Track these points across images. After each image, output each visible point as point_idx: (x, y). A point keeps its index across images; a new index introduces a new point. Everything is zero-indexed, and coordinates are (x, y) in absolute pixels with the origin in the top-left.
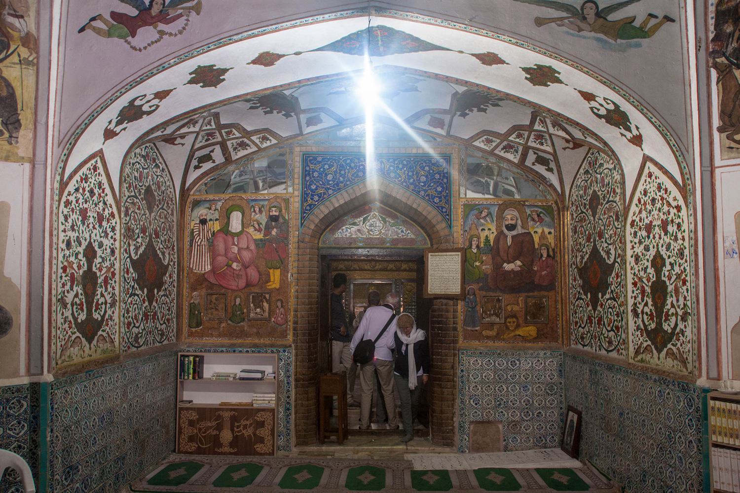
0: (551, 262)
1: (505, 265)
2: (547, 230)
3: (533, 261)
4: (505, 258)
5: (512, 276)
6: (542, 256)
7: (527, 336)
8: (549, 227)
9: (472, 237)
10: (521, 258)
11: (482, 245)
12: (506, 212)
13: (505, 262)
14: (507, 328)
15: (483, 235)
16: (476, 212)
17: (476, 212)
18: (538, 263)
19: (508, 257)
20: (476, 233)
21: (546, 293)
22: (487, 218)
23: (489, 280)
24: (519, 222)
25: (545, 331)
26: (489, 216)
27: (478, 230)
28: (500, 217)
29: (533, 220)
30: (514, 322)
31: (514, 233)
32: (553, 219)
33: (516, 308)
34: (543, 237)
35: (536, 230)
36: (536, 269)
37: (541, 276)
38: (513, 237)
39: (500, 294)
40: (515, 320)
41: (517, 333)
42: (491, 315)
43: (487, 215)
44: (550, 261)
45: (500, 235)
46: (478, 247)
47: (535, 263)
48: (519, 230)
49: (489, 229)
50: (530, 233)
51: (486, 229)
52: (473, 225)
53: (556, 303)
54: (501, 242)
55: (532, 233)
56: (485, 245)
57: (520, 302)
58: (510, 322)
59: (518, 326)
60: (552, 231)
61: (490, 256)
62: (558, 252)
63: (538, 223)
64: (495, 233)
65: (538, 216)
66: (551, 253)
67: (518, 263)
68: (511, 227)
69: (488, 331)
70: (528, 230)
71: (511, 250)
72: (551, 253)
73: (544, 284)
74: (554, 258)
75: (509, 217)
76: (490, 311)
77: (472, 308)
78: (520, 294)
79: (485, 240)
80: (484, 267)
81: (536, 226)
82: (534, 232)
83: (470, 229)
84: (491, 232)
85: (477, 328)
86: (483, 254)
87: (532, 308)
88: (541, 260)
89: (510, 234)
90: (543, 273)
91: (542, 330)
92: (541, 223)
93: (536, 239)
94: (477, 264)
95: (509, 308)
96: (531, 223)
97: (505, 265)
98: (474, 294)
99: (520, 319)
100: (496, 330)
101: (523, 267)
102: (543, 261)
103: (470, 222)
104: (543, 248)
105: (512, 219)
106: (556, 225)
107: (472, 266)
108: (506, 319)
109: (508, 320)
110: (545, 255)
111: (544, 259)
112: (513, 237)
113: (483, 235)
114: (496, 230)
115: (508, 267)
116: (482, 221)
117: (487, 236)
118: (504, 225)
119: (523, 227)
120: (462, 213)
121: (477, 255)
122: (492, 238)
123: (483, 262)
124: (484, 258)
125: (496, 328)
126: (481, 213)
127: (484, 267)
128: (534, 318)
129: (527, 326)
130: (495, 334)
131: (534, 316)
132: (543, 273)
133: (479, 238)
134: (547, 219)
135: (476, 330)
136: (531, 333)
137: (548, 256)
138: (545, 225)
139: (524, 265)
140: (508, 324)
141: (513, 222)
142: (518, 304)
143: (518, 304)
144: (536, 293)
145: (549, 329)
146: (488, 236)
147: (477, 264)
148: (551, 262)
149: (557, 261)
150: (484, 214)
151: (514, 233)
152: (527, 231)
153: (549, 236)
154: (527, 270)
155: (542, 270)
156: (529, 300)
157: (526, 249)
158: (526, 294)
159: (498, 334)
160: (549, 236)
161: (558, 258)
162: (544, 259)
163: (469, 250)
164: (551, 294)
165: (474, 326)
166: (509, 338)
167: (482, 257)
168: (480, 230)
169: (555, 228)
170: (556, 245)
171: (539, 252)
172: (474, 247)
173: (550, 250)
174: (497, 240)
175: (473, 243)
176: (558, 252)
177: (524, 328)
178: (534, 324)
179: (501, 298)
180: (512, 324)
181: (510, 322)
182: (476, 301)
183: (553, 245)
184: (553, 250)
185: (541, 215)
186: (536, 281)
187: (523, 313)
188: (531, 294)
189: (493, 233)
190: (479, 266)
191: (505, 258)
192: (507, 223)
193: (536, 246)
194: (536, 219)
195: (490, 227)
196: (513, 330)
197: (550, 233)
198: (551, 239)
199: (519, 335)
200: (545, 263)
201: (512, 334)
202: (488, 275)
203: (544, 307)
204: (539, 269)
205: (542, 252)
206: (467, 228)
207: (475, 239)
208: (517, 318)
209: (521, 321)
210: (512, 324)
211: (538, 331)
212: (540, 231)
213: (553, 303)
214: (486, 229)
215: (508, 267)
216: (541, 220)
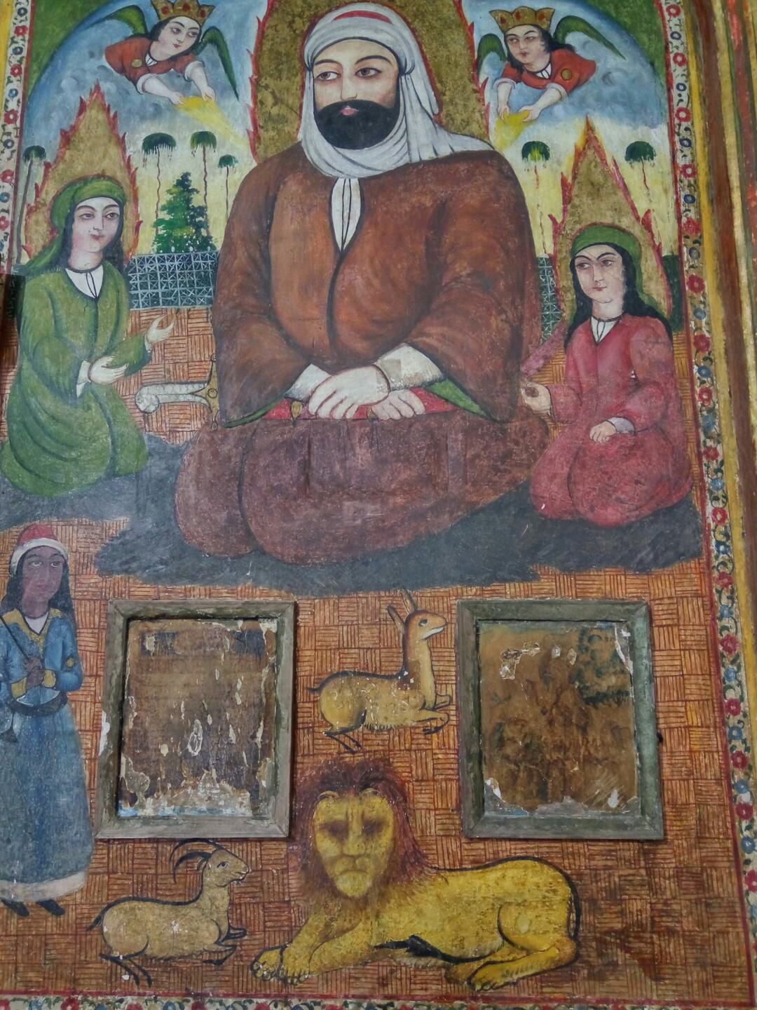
0: (657, 352)
1: (311, 378)
2: (615, 136)
3: (514, 351)
4: (316, 332)
5: (362, 456)
6: (585, 308)
7: (484, 958)
8: (633, 109)
9: (74, 190)
10: (434, 332)
11: (146, 244)
12: (327, 27)
13: (309, 357)
14: (319, 879)
15: (154, 183)
16: (115, 32)
17: (115, 32)
18: (560, 362)
19: (331, 328)
20: (110, 162)
21: (629, 586)
22: (193, 70)
23: (188, 491)
24: (418, 86)
25: (638, 906)
26: (210, 52)
27: (121, 143)
28: (285, 56)
29: (516, 70)
30: (372, 828)
31: (381, 157)
32: (659, 62)
33: (390, 707)
34: (588, 174)
35: (538, 133)
36: (541, 402)
37: (581, 455)
38: (372, 187)
39: (265, 595)
40: (378, 805)
41: (401, 921)
42: (170, 778)
43: (194, 50)
44: (648, 347)
45: (282, 169)
46: (113, 255)
47: (534, 363)
48: (417, 138)
49: (204, 138)
50: (492, 158)
51: (183, 138)
52: (94, 114)
53: (717, 660)
54: (287, 222)
55: (512, 155)
56: (164, 243)
57: (421, 654)
58: (338, 830)
59: (406, 865)
60: (658, 137)
61: (201, 322)
62: (710, 283)
63: (553, 92)
64: (246, 163)
65: (553, 44)
66: (655, 289)
67: (411, 363)
68: (357, 125)
69: (150, 914)
70: (483, 137)
71: (357, 278)
72: (655, 289)
73: (611, 514)
74: (676, 321)
75: (346, 58)
76: (179, 733)
77: (36, 712)
78: (425, 596)
79: (170, 208)
80: (148, 398)
81: (535, 110)
82: (527, 149)
83: (67, 138)
84: (214, 156)
85: (58, 889)
86: (154, 300)
87: (520, 705)
88: (579, 340)
89: (348, 167)
90: (602, 432)
91: (615, 895)
92: (571, 88)
93: (542, 195)
94: (103, 373)
95: (334, 707)
96: (500, 92)
97: (311, 378)
98: (61, 600)
99: (422, 799)
100: (222, 898)
101: (448, 390)
102: (597, 346)
103: (73, 99)
104: (593, 252)
105: (363, 72)
106: (680, 99)
107: (66, 393)
108: (301, 802)
109: (328, 809)
110: (609, 303)
111: (601, 330)
112: (372, 187)
113: (154, 183)
114: (255, 139)
115: (331, 393)
116: (154, 85)
117: (183, 183)
118: (308, 112)
119: (440, 121)
120: (23, 42)
121: (107, 308)
122: (218, 198)
123: (143, 360)
124: (155, 334)
125: (218, 878)
126: (153, 35)
127: (148, 398)
128: (543, 796)
129: (481, 865)
130: (208, 936)
131: (540, 776)
132: (602, 432)
133: (124, 196)
134: (617, 63)
135: (52, 907)
136: (522, 924)
137: (635, 305)
138: (604, 104)
139: (448, 375)
140: (326, 846)
141: (375, 91)
142: (406, 676)
143: (406, 676)
144: (548, 586)
145: (670, 886)
146: (195, 181)
147: (103, 373)
148: (657, 352)
149: (703, 343)
150: (168, 44)
151: (381, 157)
152: (475, 146)
153: (631, 173)
154: (480, 418)
155: (587, 405)
156: (496, 638)
157: (462, 269)
158: (471, 593)
159: (232, 936)
160: (631, 173)
161: (710, 316)
162: (601, 330)
163: (49, 280)
164: (663, 586)
165: (40, 869)
166: (329, 973)
167: (139, 330)
168: (135, 148)
169: (675, 120)
170: (689, 230)
171: (566, 282)
172: (85, 254)
173: (649, 266)
174: (259, 201)
175: (82, 229)
176: (710, 283)
177: (461, 884)
178: (547, 848)
179: (267, 626)
180: (354, 844)
181: (338, 830)
182: (70, 658)
183: (666, 231)
184: (671, 266)
185: (573, 39)
186: (550, 490)
187: (445, 750)
188: (511, 592)
189: (226, 161)
190: (111, 389)
191: (316, 332)
192: (329, 95)
193: (544, 244)
194: (538, 60)
195: (211, 121)
196: (362, 903)
197: (639, 152)
198: (652, 193)
199: (418, 947)
200: (609, 362)
201: (357, 939)
202: (177, 452)
203: (620, 694)
204: (566, 399)
205: (583, 278)
206: (46, 135)
207: (98, 204)
208: (397, 793)
209: (430, 821)
210: (354, 844)
211: (575, 904)
212: (564, 138)
213: (694, 660)
214: (183, 138)
215: (331, 393)
216: (572, 72)
